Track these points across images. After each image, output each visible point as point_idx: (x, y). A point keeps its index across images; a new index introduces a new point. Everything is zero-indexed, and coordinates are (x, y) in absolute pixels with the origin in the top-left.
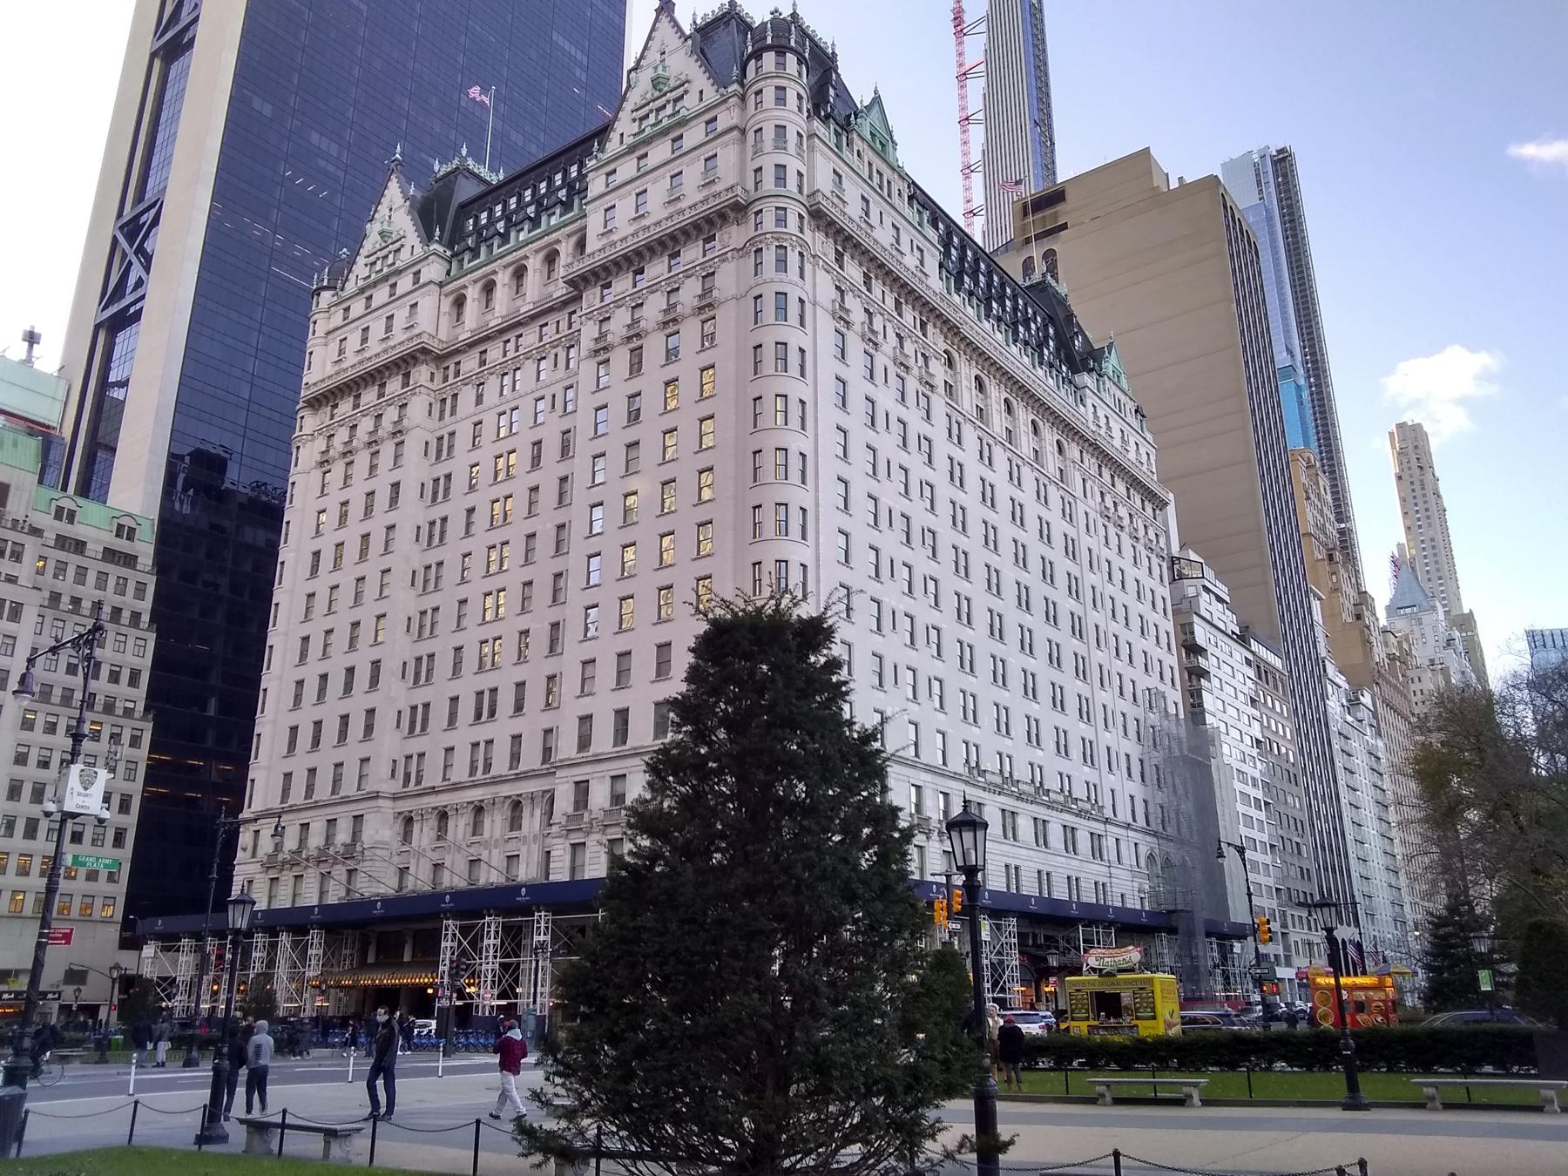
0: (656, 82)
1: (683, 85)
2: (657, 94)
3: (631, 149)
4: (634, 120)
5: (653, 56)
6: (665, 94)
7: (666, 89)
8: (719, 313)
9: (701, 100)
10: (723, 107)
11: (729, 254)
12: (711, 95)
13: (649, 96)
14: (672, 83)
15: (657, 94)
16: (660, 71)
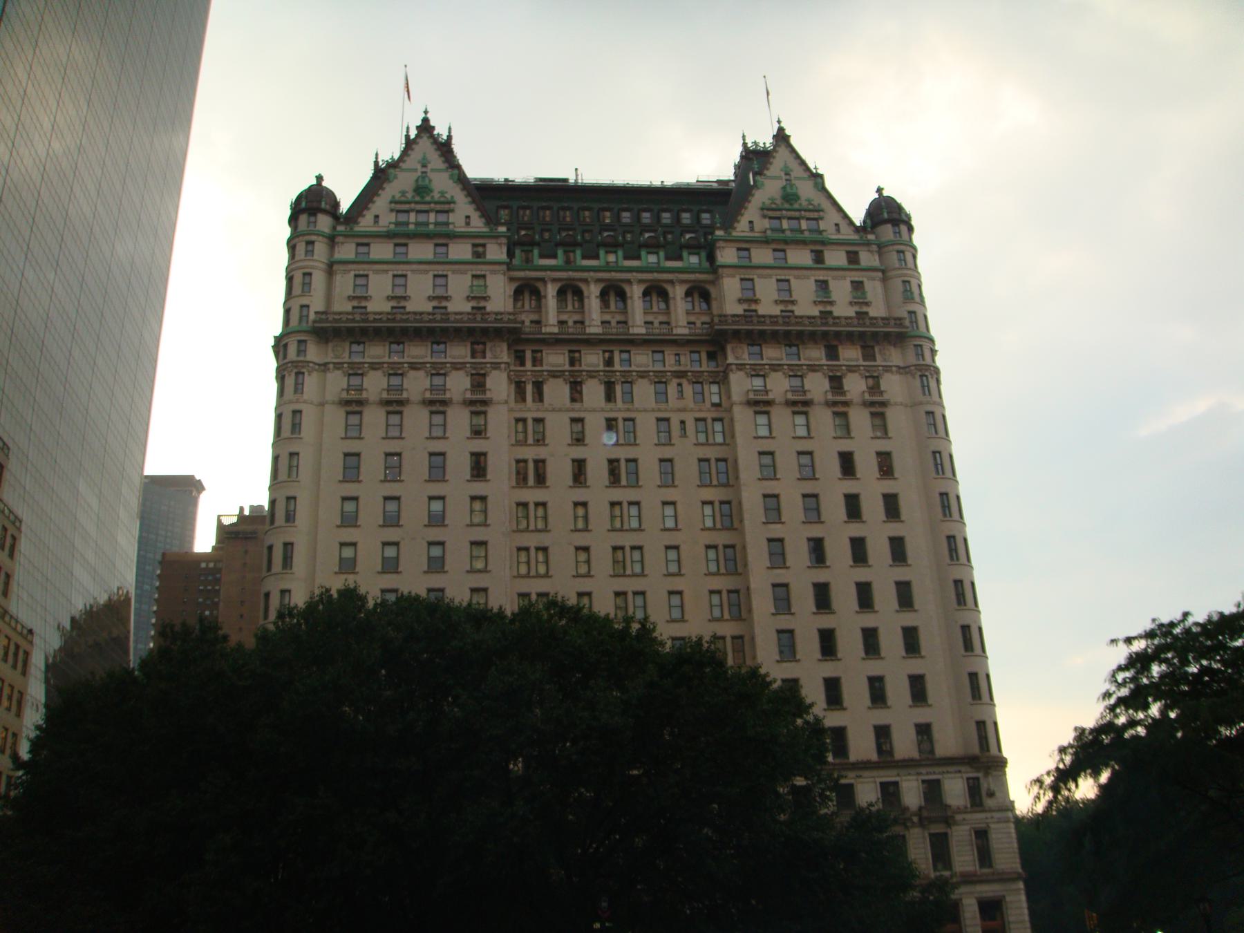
0: (422, 190)
1: (449, 203)
2: (418, 199)
3: (389, 236)
4: (392, 210)
5: (413, 161)
6: (429, 203)
7: (428, 199)
8: (491, 412)
9: (468, 224)
10: (494, 241)
11: (503, 366)
12: (478, 224)
13: (409, 196)
14: (437, 196)
15: (418, 199)
16: (427, 181)
